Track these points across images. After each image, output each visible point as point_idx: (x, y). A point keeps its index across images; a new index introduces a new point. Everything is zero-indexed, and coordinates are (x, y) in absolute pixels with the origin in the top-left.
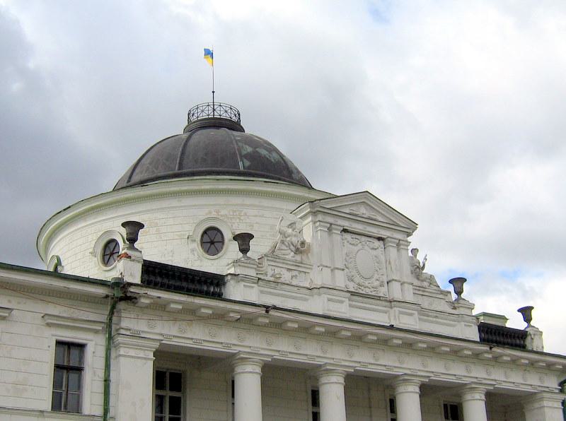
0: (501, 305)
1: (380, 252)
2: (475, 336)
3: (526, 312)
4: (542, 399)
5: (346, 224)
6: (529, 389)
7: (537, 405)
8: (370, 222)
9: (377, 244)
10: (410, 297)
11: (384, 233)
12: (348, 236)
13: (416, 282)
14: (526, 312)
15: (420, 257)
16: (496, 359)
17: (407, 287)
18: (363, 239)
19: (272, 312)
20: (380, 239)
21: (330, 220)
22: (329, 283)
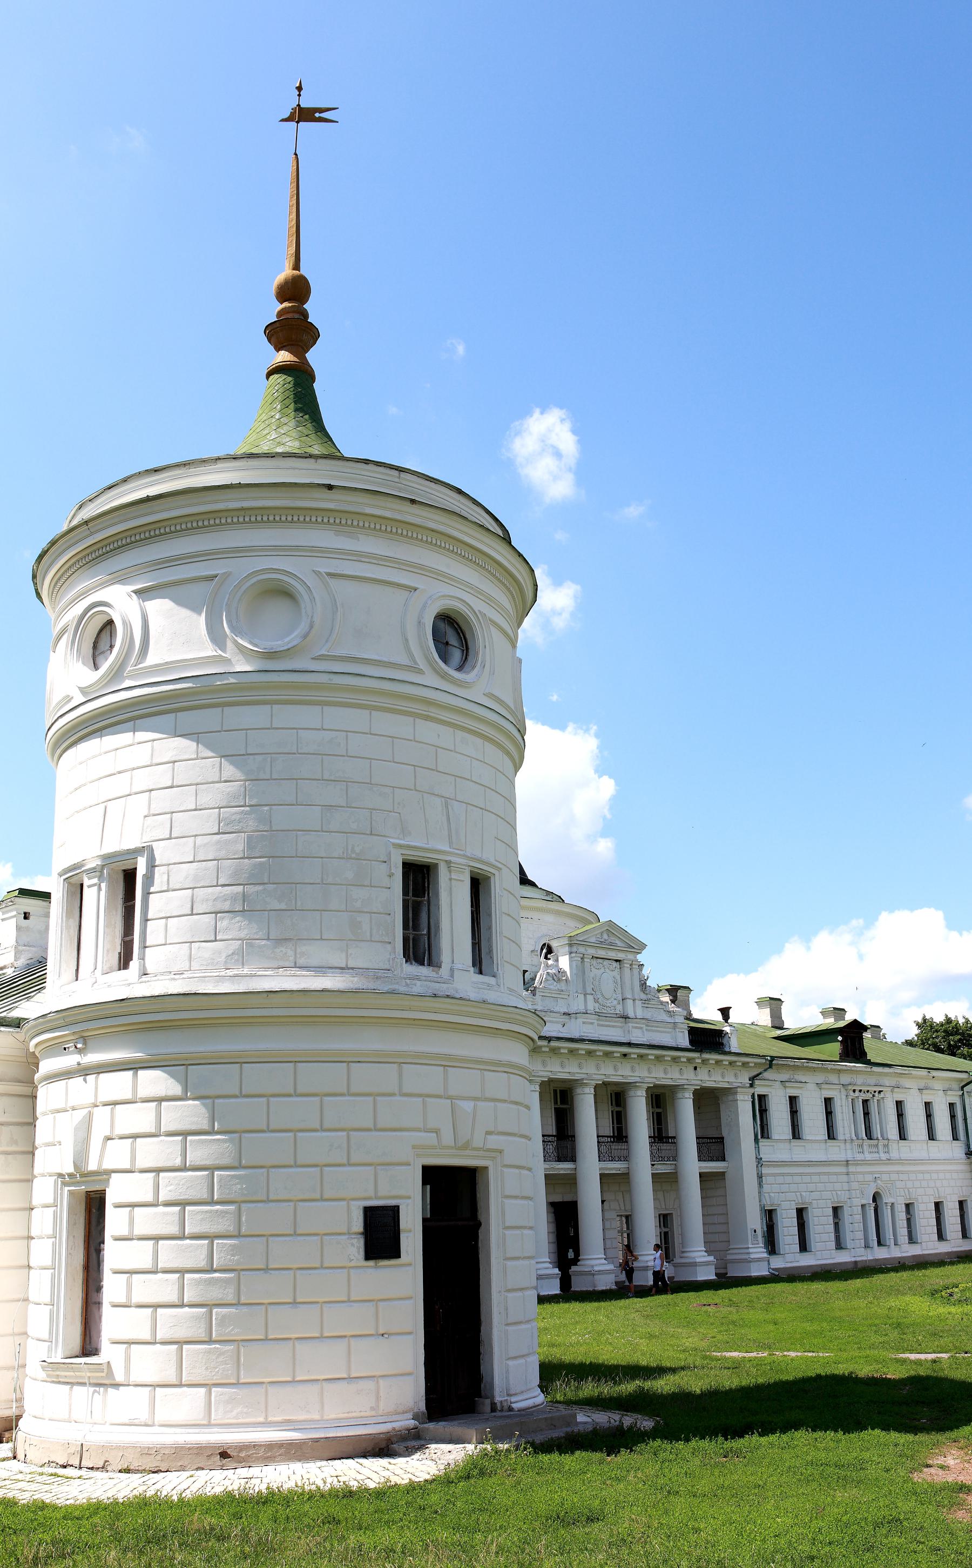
0: (705, 1010)
1: (616, 973)
2: (685, 1041)
3: (725, 1012)
4: (736, 1093)
5: (591, 951)
6: (727, 1086)
7: (731, 1098)
8: (611, 946)
9: (615, 964)
10: (640, 1014)
11: (620, 956)
12: (594, 962)
13: (643, 996)
14: (725, 1012)
15: (645, 972)
16: (704, 1062)
17: (638, 1003)
18: (606, 962)
19: (553, 1044)
20: (616, 961)
21: (582, 949)
22: (582, 1008)
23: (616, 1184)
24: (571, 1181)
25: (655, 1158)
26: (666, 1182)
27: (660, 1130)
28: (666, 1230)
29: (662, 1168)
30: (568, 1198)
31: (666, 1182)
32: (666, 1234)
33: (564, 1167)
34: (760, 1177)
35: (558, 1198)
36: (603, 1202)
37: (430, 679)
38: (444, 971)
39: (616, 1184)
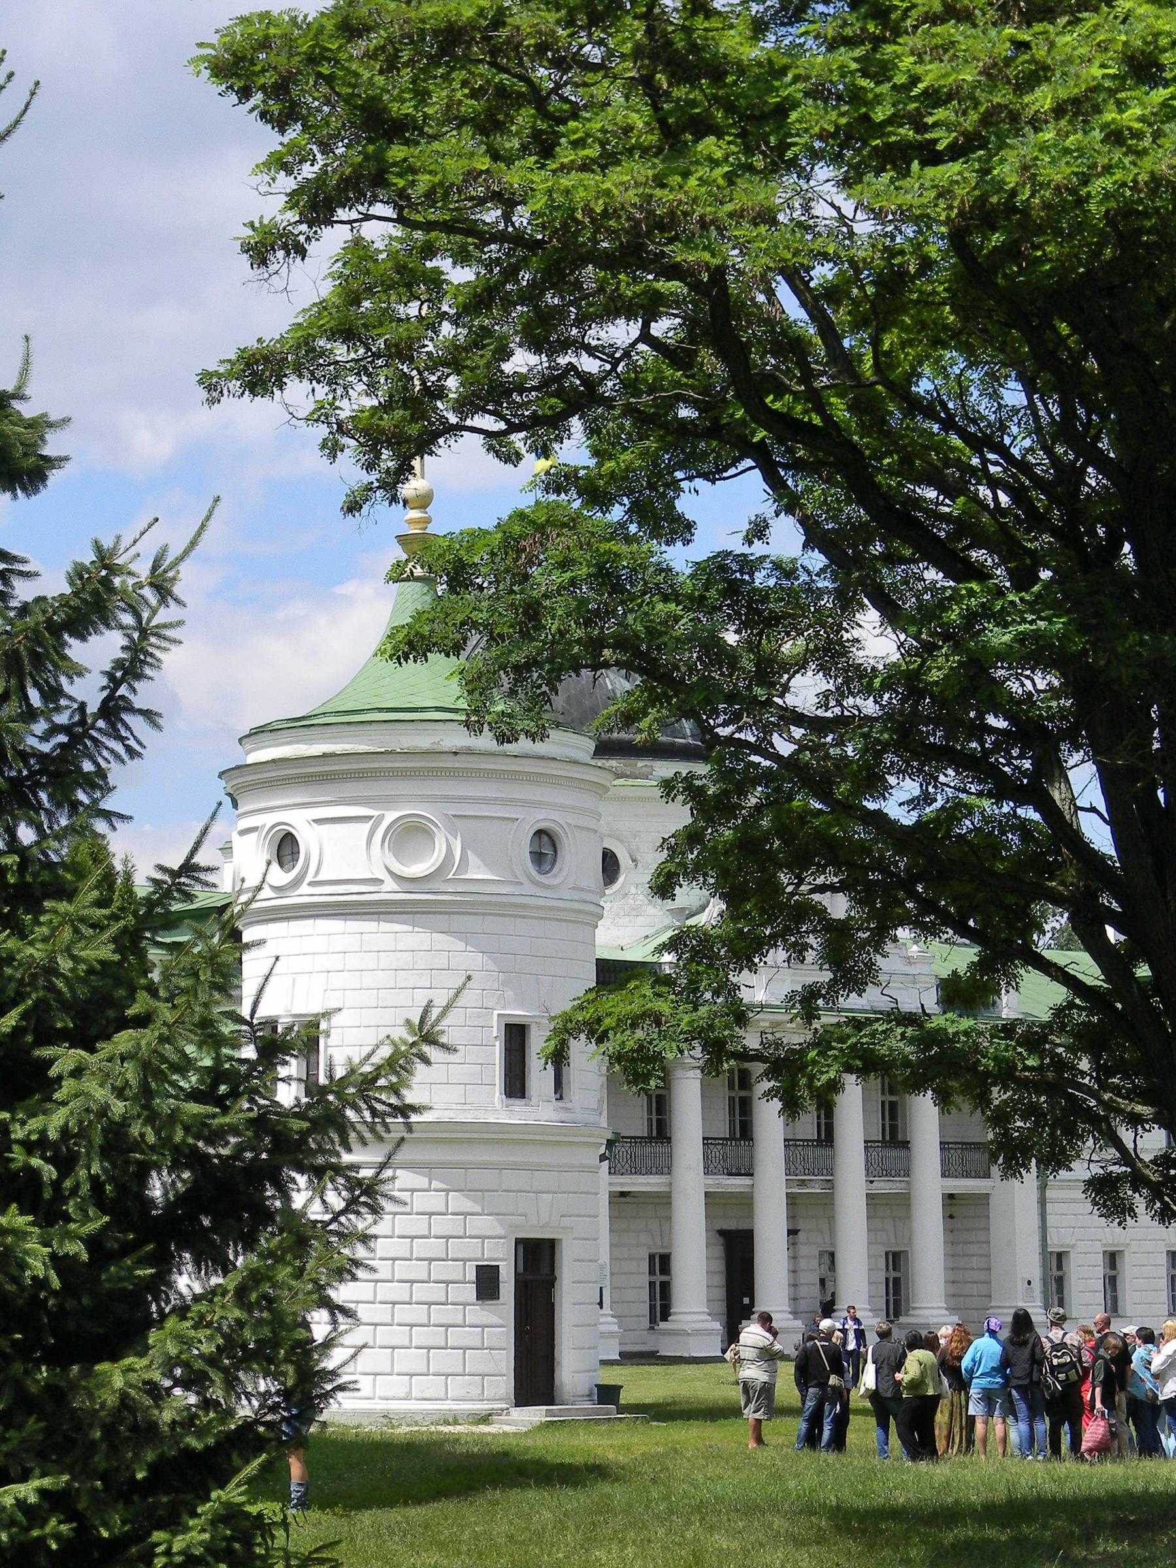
23: (810, 1210)
24: (746, 1202)
25: (873, 1170)
26: (890, 1209)
27: (894, 1130)
28: (897, 1275)
29: (882, 1186)
30: (743, 1226)
31: (890, 1209)
32: (897, 1281)
33: (737, 1184)
34: (1043, 1202)
35: (731, 1225)
36: (792, 1232)
37: (529, 889)
38: (534, 1100)
39: (810, 1210)
